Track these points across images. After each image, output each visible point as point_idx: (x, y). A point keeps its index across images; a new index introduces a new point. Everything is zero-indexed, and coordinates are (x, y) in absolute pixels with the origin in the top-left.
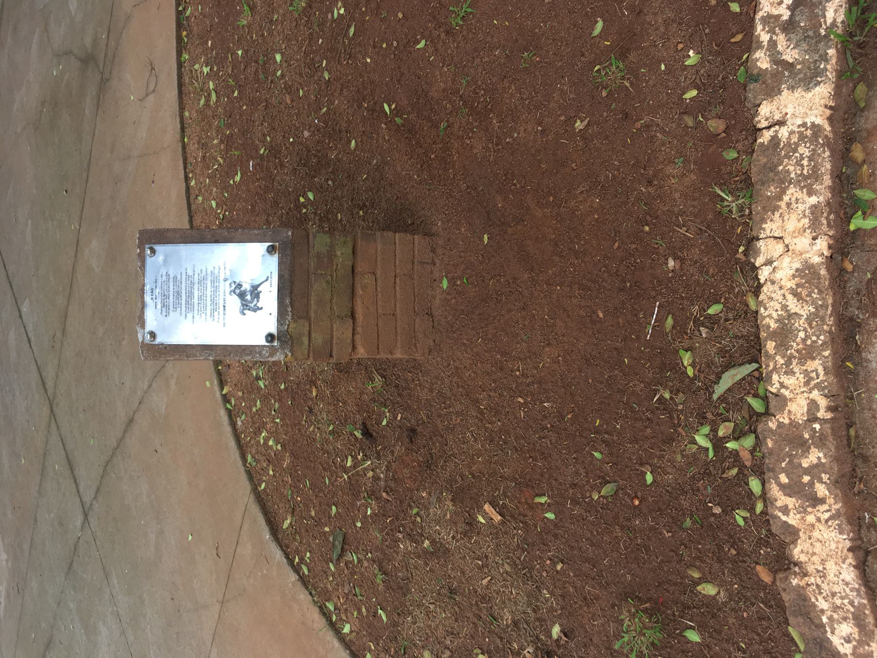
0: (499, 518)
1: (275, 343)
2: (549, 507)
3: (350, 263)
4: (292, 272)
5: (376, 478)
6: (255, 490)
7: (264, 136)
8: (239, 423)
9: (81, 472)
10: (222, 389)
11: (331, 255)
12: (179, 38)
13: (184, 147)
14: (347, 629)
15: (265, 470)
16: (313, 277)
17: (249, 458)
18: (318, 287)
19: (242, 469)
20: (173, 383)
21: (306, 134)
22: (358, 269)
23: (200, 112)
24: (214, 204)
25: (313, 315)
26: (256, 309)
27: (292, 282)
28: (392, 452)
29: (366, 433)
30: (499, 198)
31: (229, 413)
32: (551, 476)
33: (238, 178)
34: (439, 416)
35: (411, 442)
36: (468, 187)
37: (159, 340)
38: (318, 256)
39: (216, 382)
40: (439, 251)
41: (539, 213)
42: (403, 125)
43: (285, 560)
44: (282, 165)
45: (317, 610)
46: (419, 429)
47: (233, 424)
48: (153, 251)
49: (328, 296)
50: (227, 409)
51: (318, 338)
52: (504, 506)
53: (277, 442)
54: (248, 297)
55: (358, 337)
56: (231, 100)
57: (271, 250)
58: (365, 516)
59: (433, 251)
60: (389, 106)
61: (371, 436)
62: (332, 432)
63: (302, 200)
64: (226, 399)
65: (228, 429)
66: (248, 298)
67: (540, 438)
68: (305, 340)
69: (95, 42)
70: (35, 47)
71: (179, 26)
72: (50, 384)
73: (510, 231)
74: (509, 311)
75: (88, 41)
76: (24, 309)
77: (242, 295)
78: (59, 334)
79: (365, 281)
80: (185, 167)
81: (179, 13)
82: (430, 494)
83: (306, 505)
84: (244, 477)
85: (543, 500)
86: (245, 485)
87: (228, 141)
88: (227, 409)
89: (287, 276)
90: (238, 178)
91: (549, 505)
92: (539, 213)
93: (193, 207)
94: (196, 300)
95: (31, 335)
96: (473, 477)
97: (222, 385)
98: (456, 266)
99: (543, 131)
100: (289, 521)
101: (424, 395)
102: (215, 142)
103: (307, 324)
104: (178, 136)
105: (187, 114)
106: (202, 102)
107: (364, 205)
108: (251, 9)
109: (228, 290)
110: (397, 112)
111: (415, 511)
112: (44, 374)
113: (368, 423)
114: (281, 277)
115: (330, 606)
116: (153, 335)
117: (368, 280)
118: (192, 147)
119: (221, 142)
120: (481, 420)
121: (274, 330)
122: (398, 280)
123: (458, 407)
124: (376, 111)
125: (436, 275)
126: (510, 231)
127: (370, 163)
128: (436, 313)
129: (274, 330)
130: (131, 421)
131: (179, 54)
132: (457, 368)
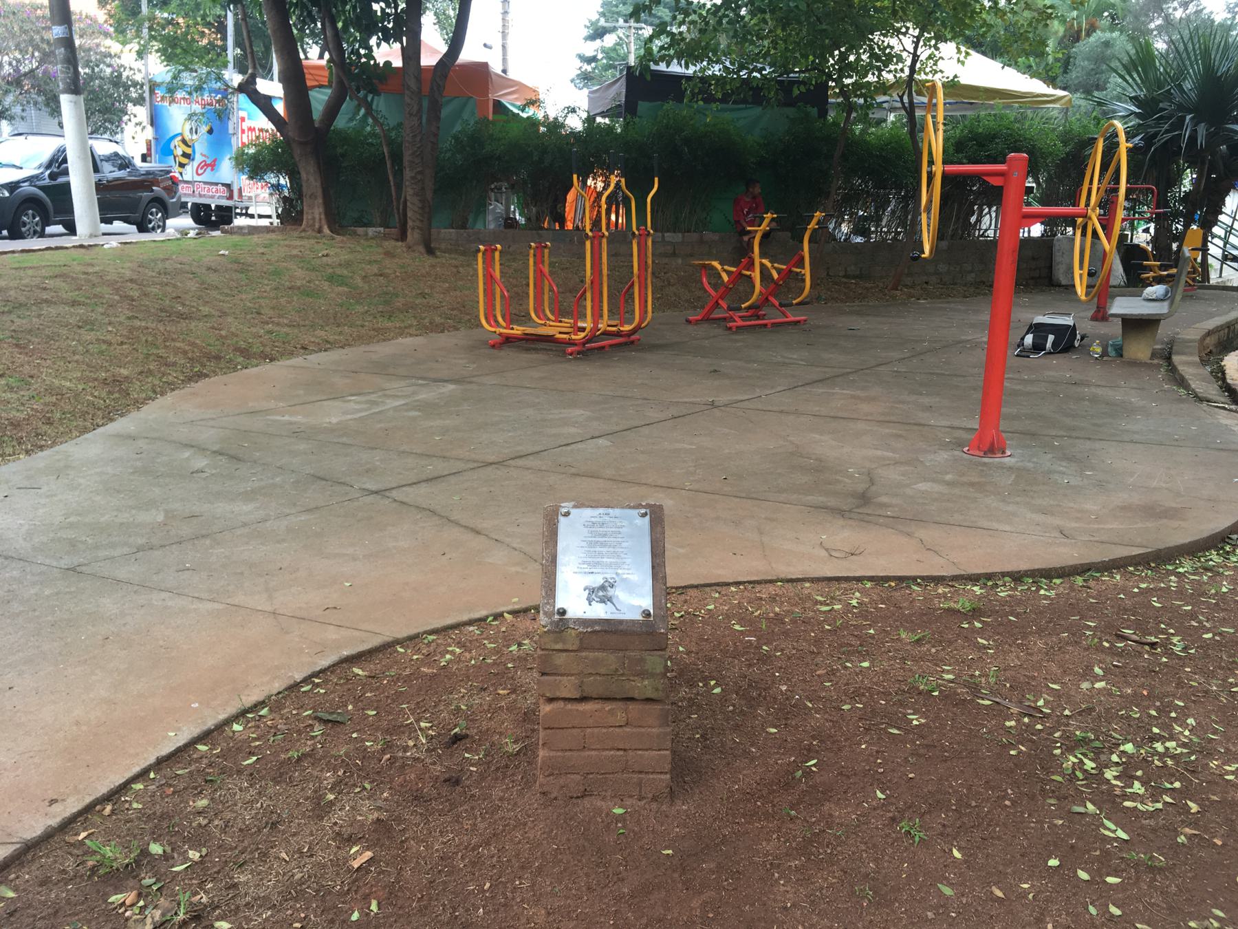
0: (356, 866)
1: (557, 617)
2: (366, 914)
3: (636, 696)
4: (624, 633)
5: (406, 748)
6: (398, 642)
7: (782, 650)
8: (471, 628)
9: (423, 489)
10: (509, 613)
11: (643, 674)
12: (887, 579)
13: (771, 582)
15: (418, 651)
16: (621, 654)
17: (431, 638)
18: (611, 660)
19: (421, 630)
20: (519, 569)
21: (784, 688)
22: (632, 706)
23: (809, 597)
24: (712, 607)
25: (584, 654)
26: (590, 601)
27: (615, 632)
28: (434, 763)
29: (457, 739)
30: (712, 866)
31: (483, 619)
32: (400, 916)
33: (737, 627)
34: (472, 808)
35: (445, 781)
36: (725, 836)
37: (561, 519)
38: (641, 660)
39: (517, 607)
40: (654, 806)
41: (695, 903)
42: (793, 778)
43: (318, 669)
44: (750, 666)
45: (261, 699)
46: (458, 789)
47: (470, 623)
48: (644, 515)
49: (603, 671)
50: (487, 617)
51: (560, 660)
52: (368, 872)
53: (448, 662)
54: (601, 593)
55: (561, 704)
56: (820, 623)
57: (647, 614)
58: (363, 741)
59: (654, 799)
60: (814, 765)
61: (454, 743)
62: (458, 709)
63: (713, 683)
64: (498, 616)
65: (465, 618)
66: (600, 593)
67: (444, 905)
68: (559, 646)
70: (879, 453)
71: (900, 579)
72: (520, 462)
73: (676, 875)
74: (587, 875)
75: (884, 499)
76: (600, 441)
77: (603, 588)
78: (573, 470)
79: (619, 712)
80: (750, 582)
81: (914, 579)
82: (386, 800)
83: (377, 689)
84: (412, 631)
85: (374, 907)
86: (403, 633)
87: (779, 619)
88: (487, 617)
89: (621, 627)
90: (737, 627)
91: (368, 914)
92: (695, 903)
93: (708, 589)
94: (598, 549)
96: (402, 842)
97: (514, 613)
98: (638, 822)
99: (785, 908)
100: (360, 672)
101: (496, 793)
102: (777, 609)
103: (575, 647)
104: (783, 576)
105: (807, 585)
106: (819, 598)
107: (706, 739)
108: (918, 640)
109: (608, 576)
110: (808, 773)
111: (368, 786)
112: (531, 458)
113: (467, 741)
114: (621, 622)
115: (264, 712)
116: (567, 514)
117: (620, 717)
118: (771, 589)
119: (776, 614)
120: (466, 848)
121: (569, 615)
122: (621, 753)
123: (482, 826)
124: (809, 752)
125: (628, 802)
126: (676, 875)
127: (752, 745)
128: (586, 802)
129: (567, 616)
131: (871, 579)
132: (525, 824)
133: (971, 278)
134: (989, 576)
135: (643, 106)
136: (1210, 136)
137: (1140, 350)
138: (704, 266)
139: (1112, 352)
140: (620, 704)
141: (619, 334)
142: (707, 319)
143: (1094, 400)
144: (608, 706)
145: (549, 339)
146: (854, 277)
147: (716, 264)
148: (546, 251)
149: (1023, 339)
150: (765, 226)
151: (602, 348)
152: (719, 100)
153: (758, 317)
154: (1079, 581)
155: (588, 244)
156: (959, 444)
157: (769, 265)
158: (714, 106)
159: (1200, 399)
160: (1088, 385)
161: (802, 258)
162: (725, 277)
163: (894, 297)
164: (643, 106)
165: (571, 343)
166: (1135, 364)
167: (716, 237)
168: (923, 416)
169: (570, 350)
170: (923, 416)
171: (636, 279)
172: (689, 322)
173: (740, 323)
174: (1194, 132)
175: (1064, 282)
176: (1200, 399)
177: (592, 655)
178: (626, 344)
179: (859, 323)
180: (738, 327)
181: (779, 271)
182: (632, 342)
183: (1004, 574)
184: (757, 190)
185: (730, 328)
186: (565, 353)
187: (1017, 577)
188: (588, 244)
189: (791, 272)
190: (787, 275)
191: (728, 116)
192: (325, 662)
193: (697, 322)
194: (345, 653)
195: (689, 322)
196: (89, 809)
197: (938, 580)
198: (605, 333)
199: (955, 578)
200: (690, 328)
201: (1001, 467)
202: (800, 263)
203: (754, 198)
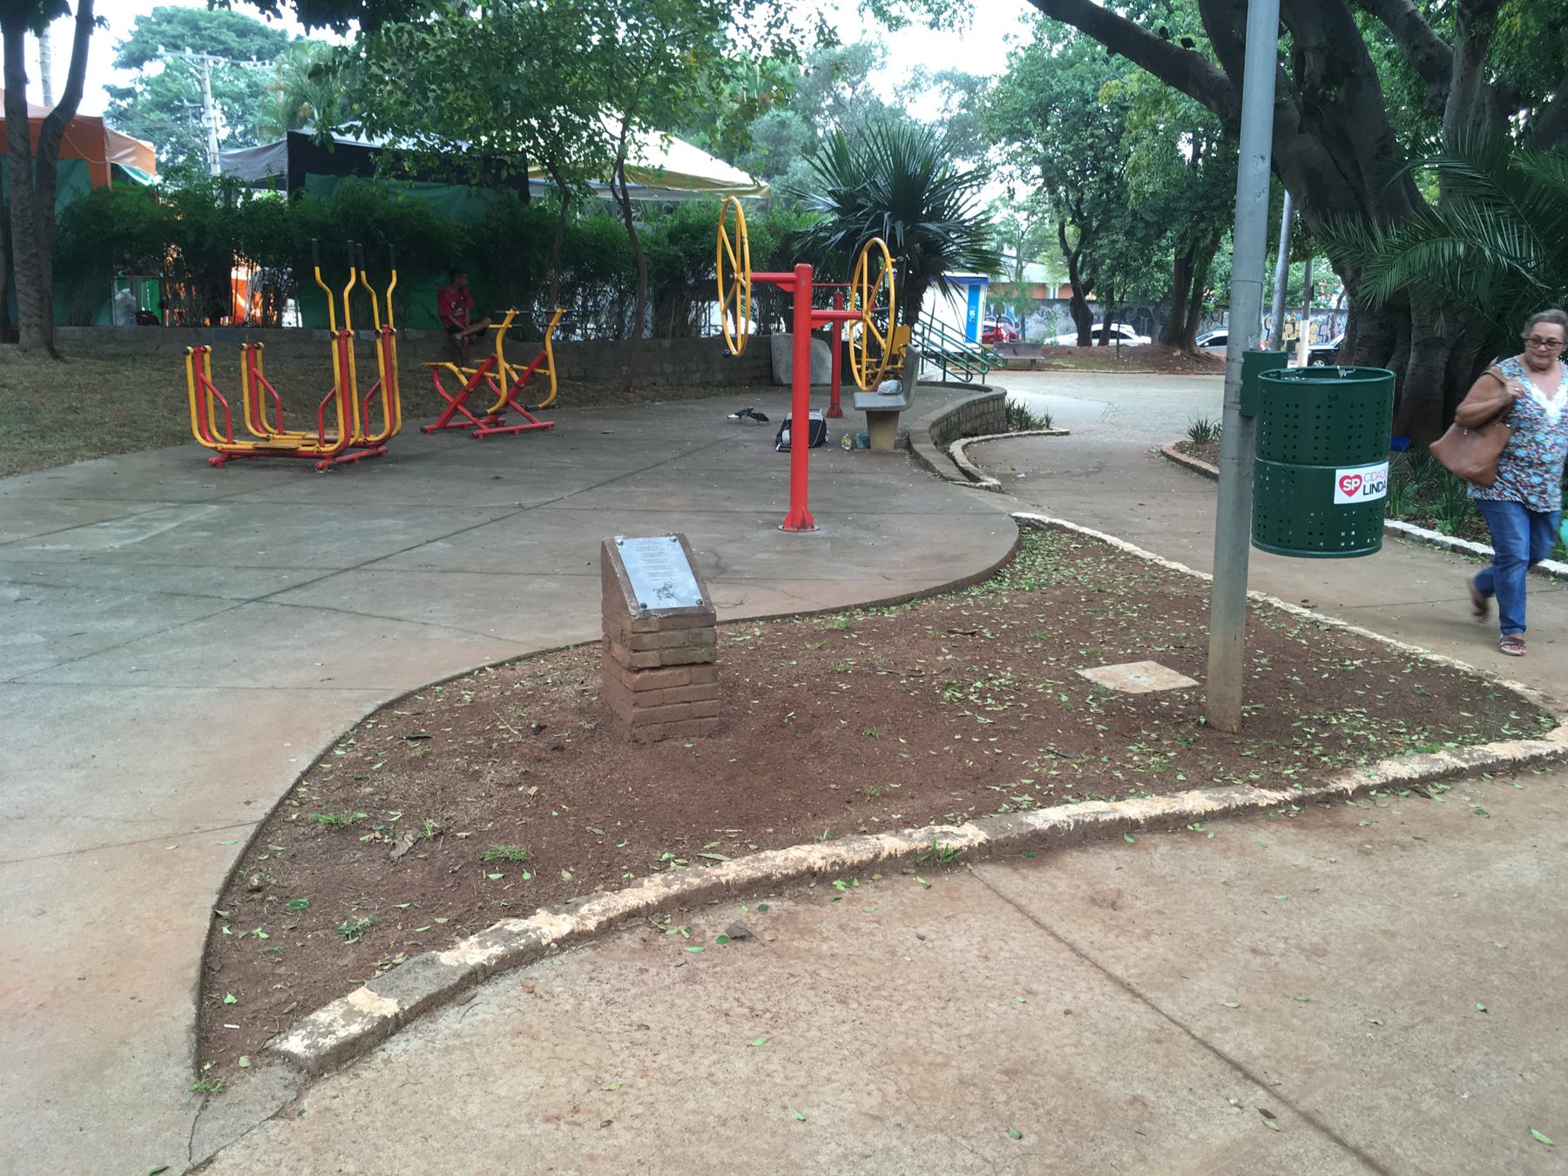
6: (413, 693)
11: (701, 645)
12: (773, 618)
14: (339, 752)
18: (680, 635)
22: (694, 669)
47: (462, 676)
59: (710, 736)
64: (482, 670)
65: (456, 673)
69: (738, 572)
71: (783, 617)
72: (371, 566)
75: (738, 568)
76: (440, 544)
79: (684, 674)
81: (793, 615)
95: (415, 551)
110: (791, 719)
117: (686, 679)
124: (786, 711)
128: (665, 743)
130: (398, 620)
131: (761, 619)
133: (696, 377)
134: (846, 609)
135: (312, 179)
136: (907, 234)
137: (884, 440)
138: (436, 368)
139: (861, 445)
140: (686, 669)
141: (365, 445)
142: (443, 428)
143: (862, 484)
144: (678, 671)
145: (290, 453)
146: (579, 379)
147: (450, 365)
148: (259, 353)
149: (780, 435)
150: (507, 323)
151: (351, 461)
152: (414, 179)
153: (498, 425)
154: (908, 607)
155: (335, 344)
156: (774, 525)
157: (455, 369)
158: (407, 183)
159: (946, 479)
160: (852, 473)
161: (546, 358)
162: (465, 381)
163: (628, 400)
164: (312, 179)
165: (319, 456)
166: (882, 453)
167: (421, 335)
168: (728, 505)
169: (321, 463)
170: (728, 505)
171: (383, 383)
172: (425, 431)
173: (487, 430)
174: (893, 229)
175: (785, 381)
176: (946, 479)
177: (667, 634)
178: (372, 456)
179: (610, 427)
180: (485, 435)
181: (468, 376)
182: (380, 454)
183: (856, 606)
184: (465, 281)
185: (477, 437)
186: (312, 469)
187: (865, 608)
188: (335, 344)
189: (533, 373)
190: (529, 378)
191: (425, 194)
192: (370, 709)
193: (432, 432)
194: (380, 702)
195: (425, 431)
196: (281, 803)
197: (811, 615)
198: (356, 445)
199: (823, 612)
200: (430, 439)
201: (816, 538)
202: (544, 363)
203: (461, 289)
